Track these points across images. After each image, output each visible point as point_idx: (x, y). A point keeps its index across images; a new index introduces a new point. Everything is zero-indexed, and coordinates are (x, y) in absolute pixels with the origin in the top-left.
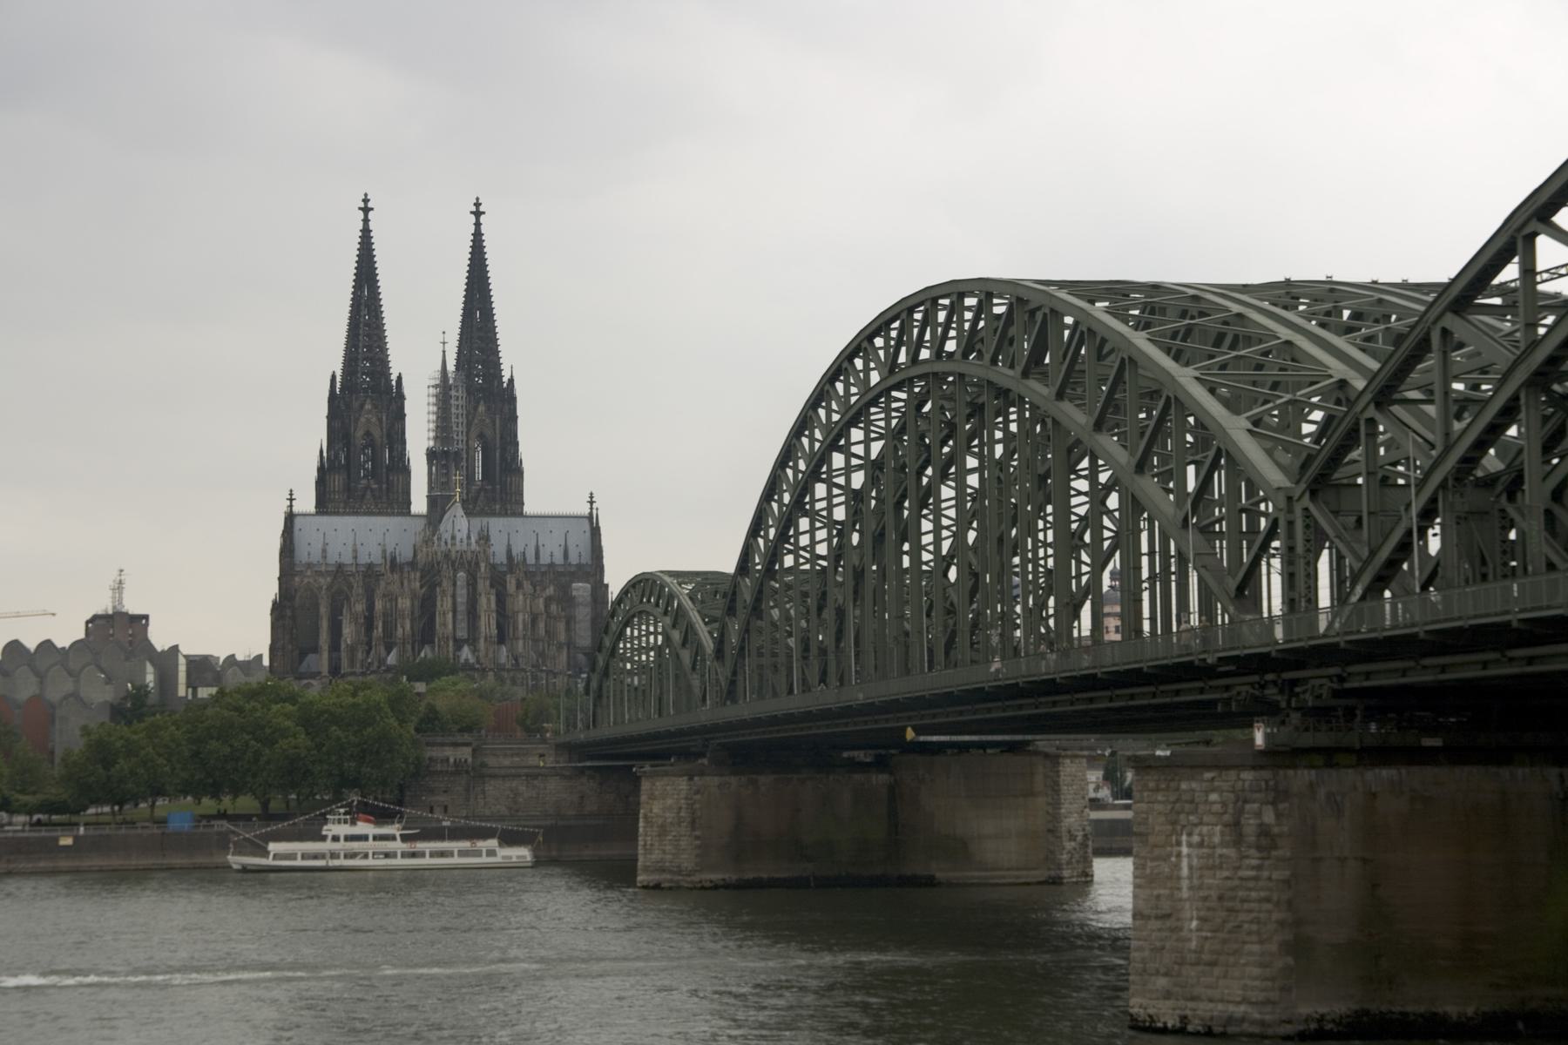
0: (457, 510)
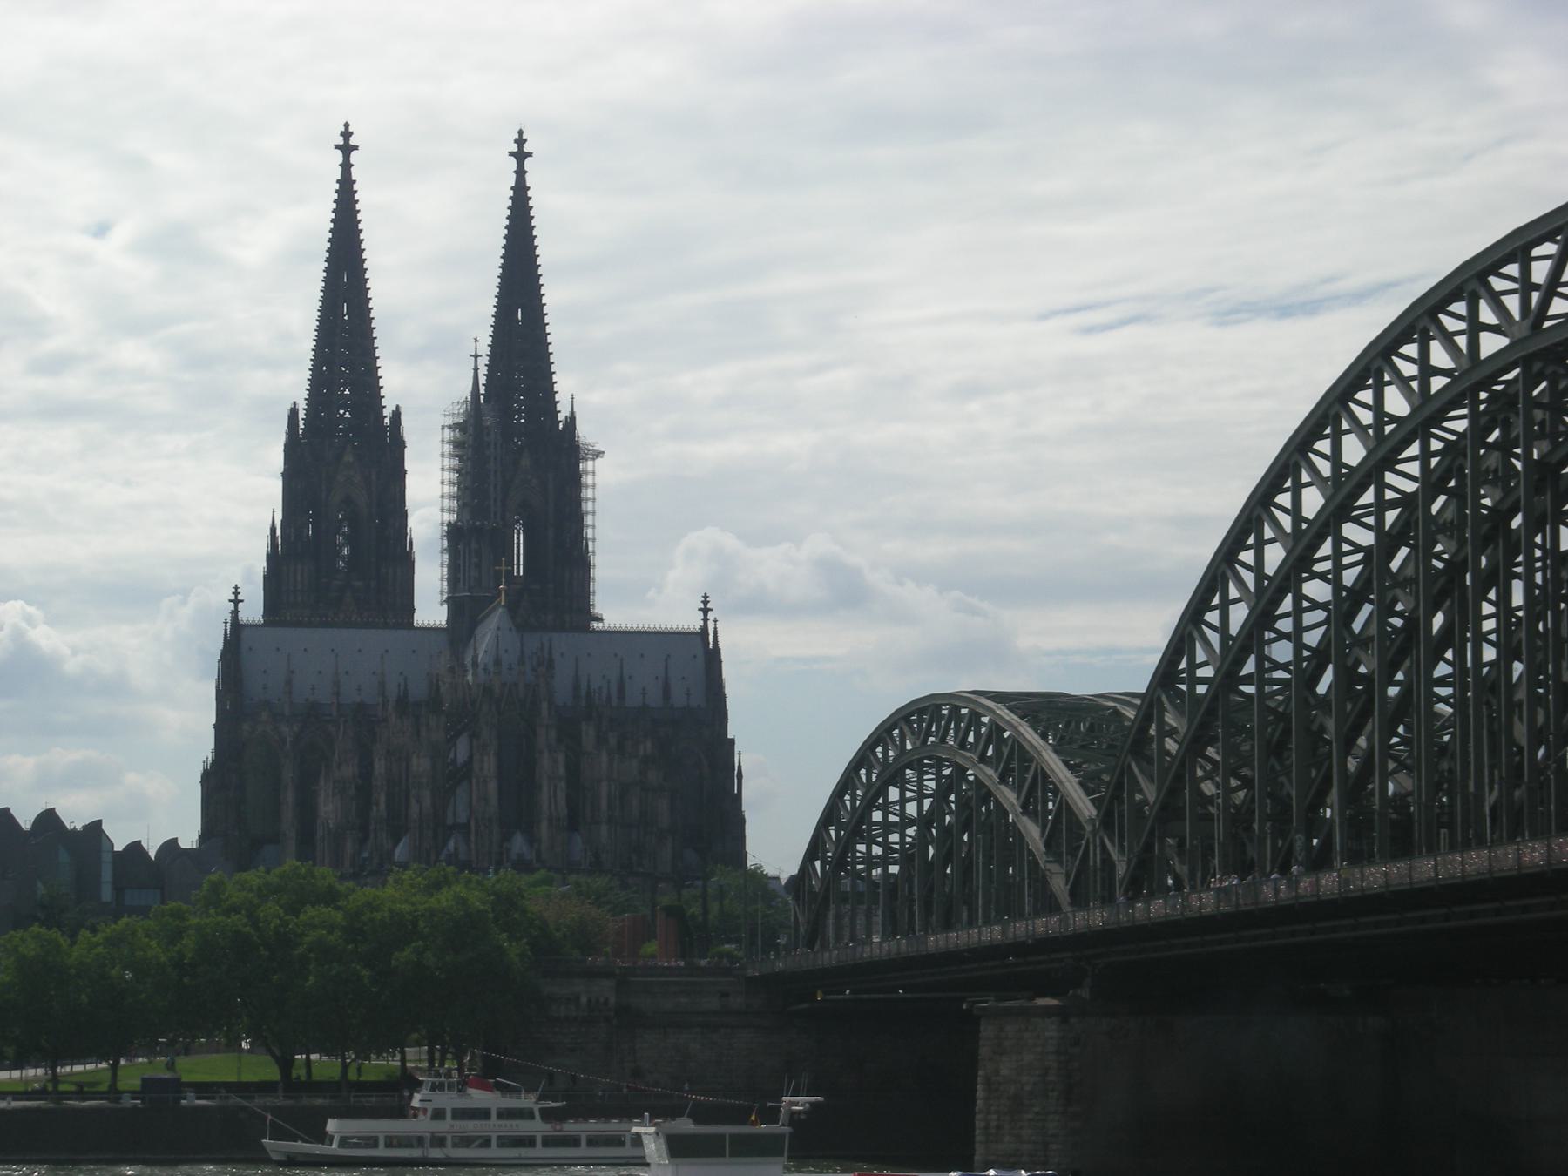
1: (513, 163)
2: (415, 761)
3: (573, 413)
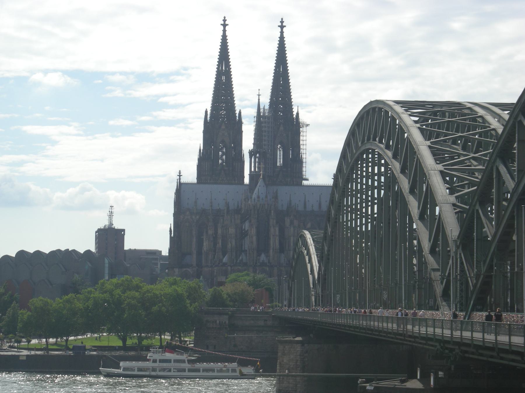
0: (261, 182)
1: (279, 29)
2: (230, 229)
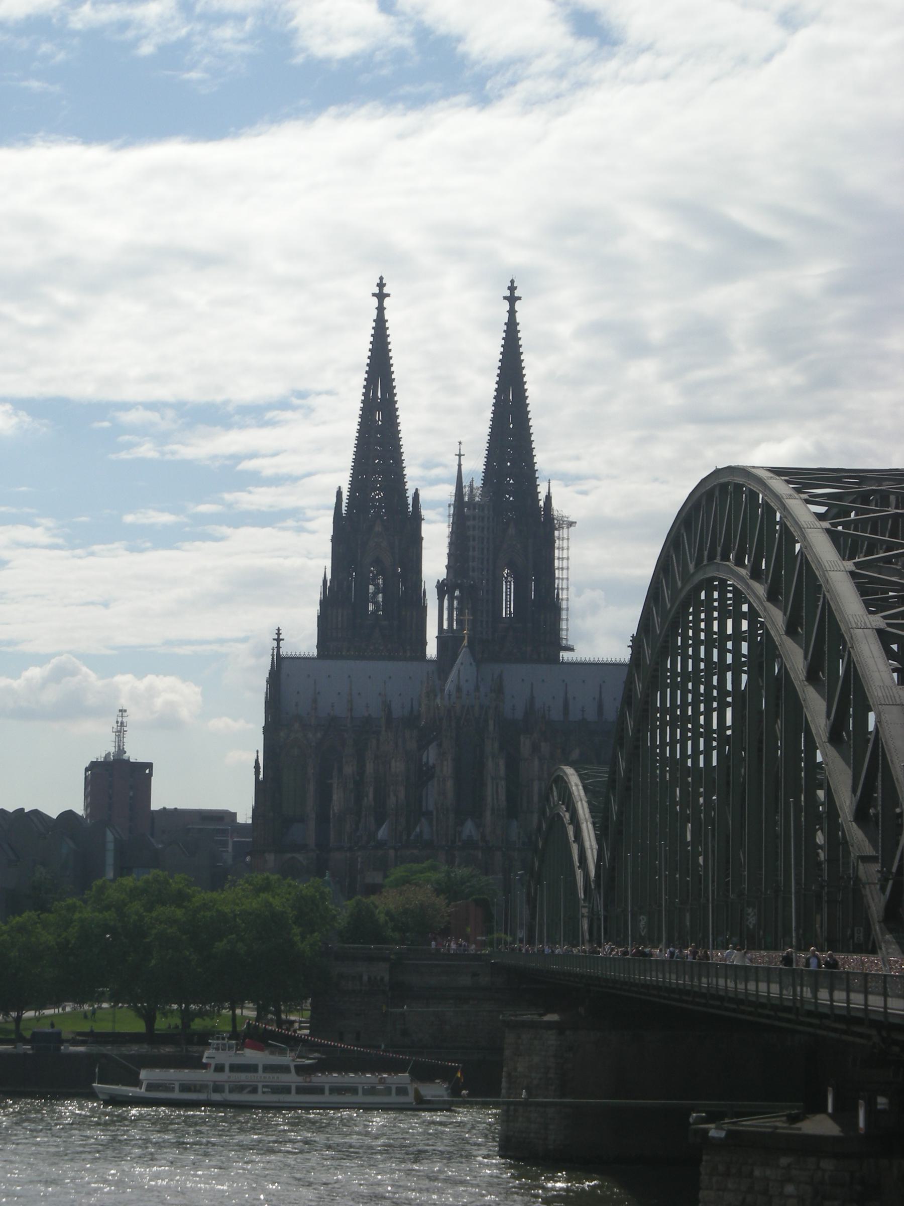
0: (464, 655)
2: (393, 763)
3: (549, 493)
